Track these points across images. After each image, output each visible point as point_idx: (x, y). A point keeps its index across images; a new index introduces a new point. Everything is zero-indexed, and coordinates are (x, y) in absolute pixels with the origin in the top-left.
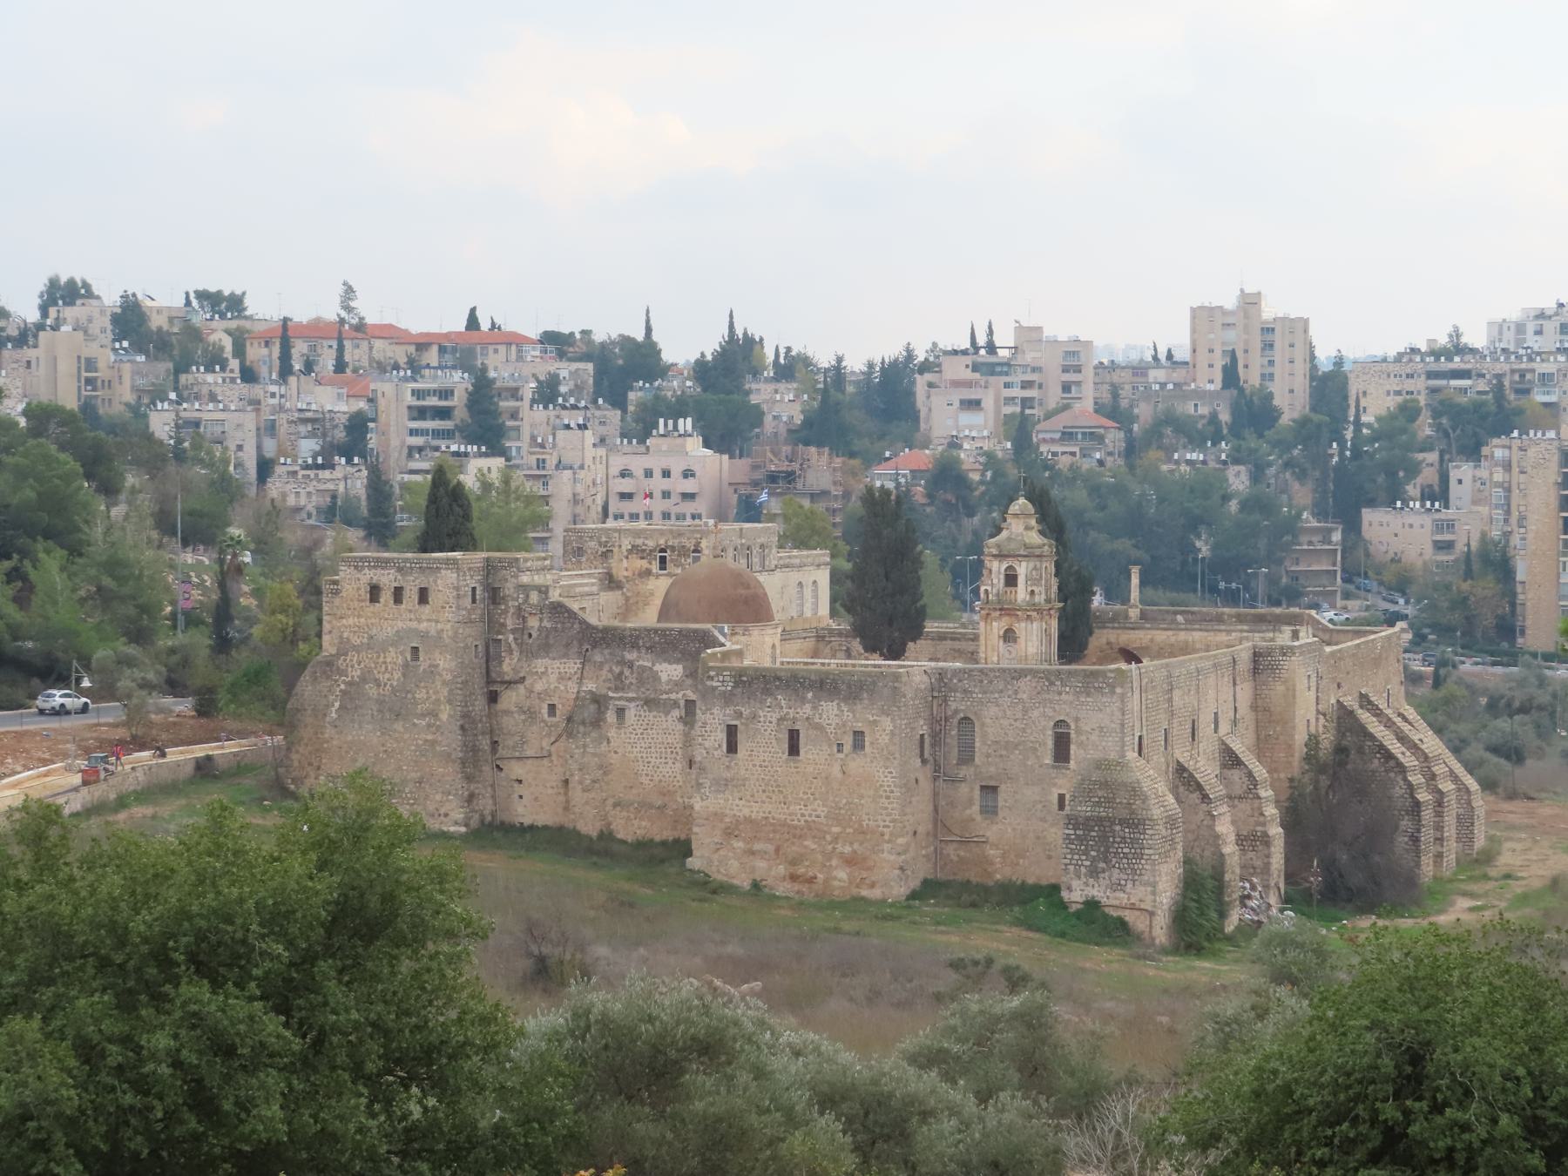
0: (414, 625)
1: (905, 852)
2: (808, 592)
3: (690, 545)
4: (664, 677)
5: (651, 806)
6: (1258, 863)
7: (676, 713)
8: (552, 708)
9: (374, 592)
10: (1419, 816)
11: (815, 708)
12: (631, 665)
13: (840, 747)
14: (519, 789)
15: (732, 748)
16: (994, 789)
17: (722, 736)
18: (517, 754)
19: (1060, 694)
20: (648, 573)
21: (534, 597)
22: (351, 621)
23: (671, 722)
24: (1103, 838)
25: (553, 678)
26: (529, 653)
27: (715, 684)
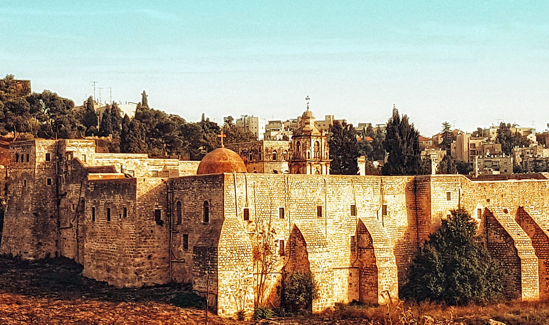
1: (139, 265)
6: (374, 281)
10: (520, 266)
18: (65, 227)
19: (205, 188)
24: (204, 257)
26: (68, 182)
27: (90, 189)
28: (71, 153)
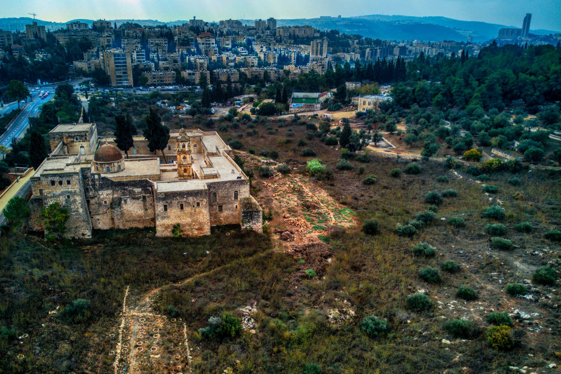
0: (67, 190)
3: (84, 134)
4: (136, 192)
5: (136, 220)
7: (141, 199)
8: (105, 202)
11: (187, 199)
12: (127, 190)
13: (194, 206)
14: (100, 221)
16: (222, 206)
17: (163, 207)
20: (73, 141)
22: (46, 191)
23: (140, 201)
25: (105, 195)
26: (96, 190)
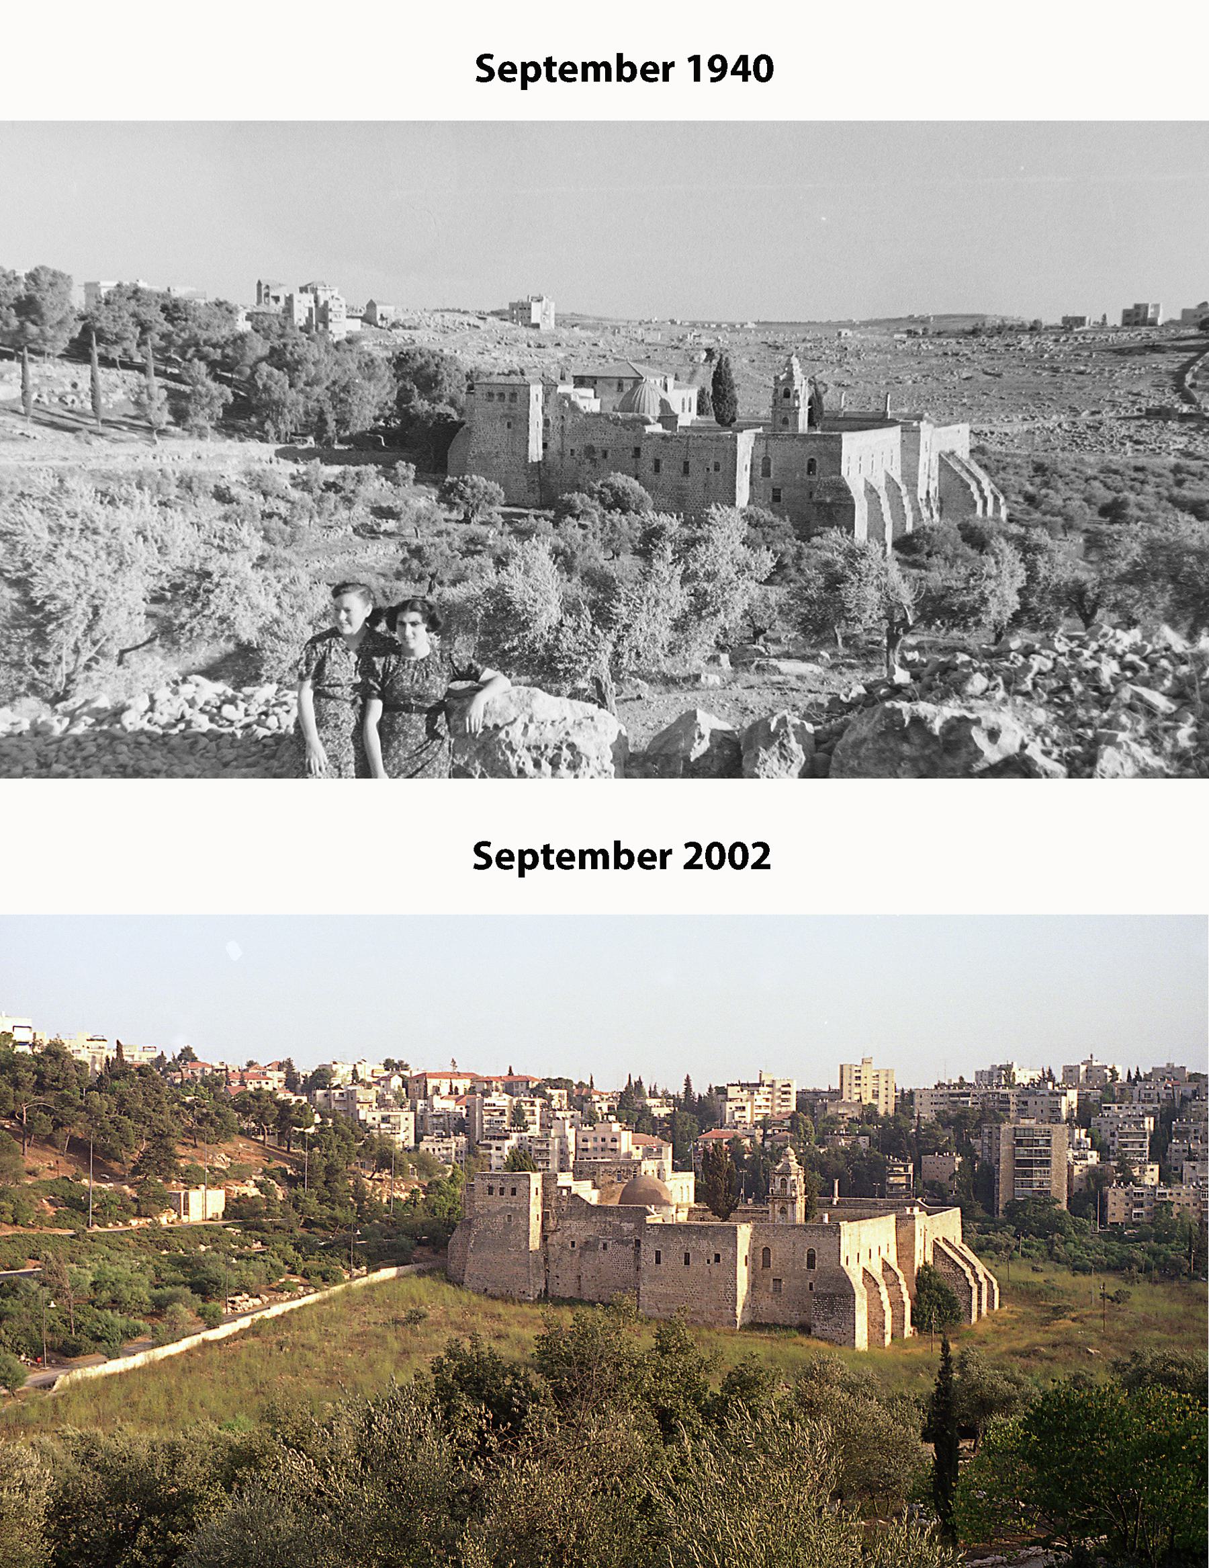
2: (685, 1190)
8: (573, 1243)
9: (491, 1190)
15: (658, 1262)
21: (565, 1192)
26: (561, 1217)
28: (569, 1189)
